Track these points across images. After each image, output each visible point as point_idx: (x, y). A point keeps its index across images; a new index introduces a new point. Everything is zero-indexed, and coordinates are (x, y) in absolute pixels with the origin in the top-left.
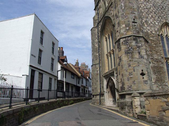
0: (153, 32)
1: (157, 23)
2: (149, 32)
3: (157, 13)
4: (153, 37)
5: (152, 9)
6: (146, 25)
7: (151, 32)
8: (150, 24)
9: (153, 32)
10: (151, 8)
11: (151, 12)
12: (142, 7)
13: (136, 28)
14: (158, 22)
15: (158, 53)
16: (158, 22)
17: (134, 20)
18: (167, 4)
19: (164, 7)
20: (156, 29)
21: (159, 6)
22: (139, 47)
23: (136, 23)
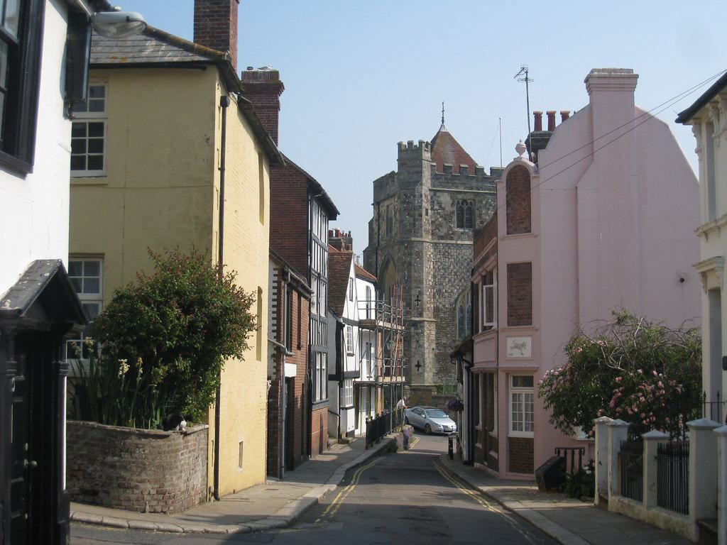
4: (445, 313)
5: (452, 267)
6: (437, 297)
8: (443, 293)
13: (418, 309)
20: (452, 300)
22: (417, 334)
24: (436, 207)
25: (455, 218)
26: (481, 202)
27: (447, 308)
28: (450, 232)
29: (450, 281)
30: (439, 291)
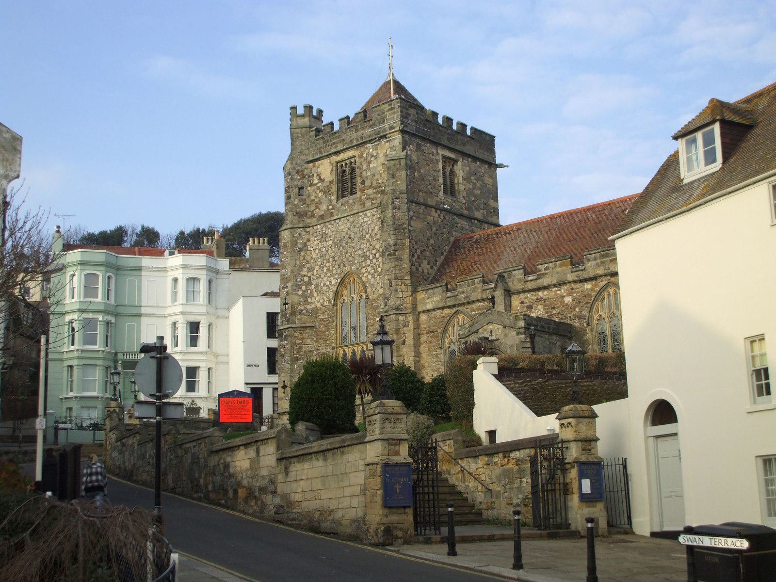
0: (325, 304)
1: (334, 282)
2: (319, 305)
3: (336, 258)
5: (330, 252)
7: (322, 304)
9: (325, 304)
10: (327, 251)
11: (328, 261)
12: (314, 257)
14: (337, 276)
15: (328, 342)
16: (337, 276)
17: (285, 299)
18: (358, 225)
19: (352, 237)
20: (331, 295)
21: (344, 237)
23: (287, 304)
24: (316, 181)
25: (334, 188)
26: (361, 156)
27: (325, 306)
28: (330, 207)
29: (328, 270)
30: (317, 286)
